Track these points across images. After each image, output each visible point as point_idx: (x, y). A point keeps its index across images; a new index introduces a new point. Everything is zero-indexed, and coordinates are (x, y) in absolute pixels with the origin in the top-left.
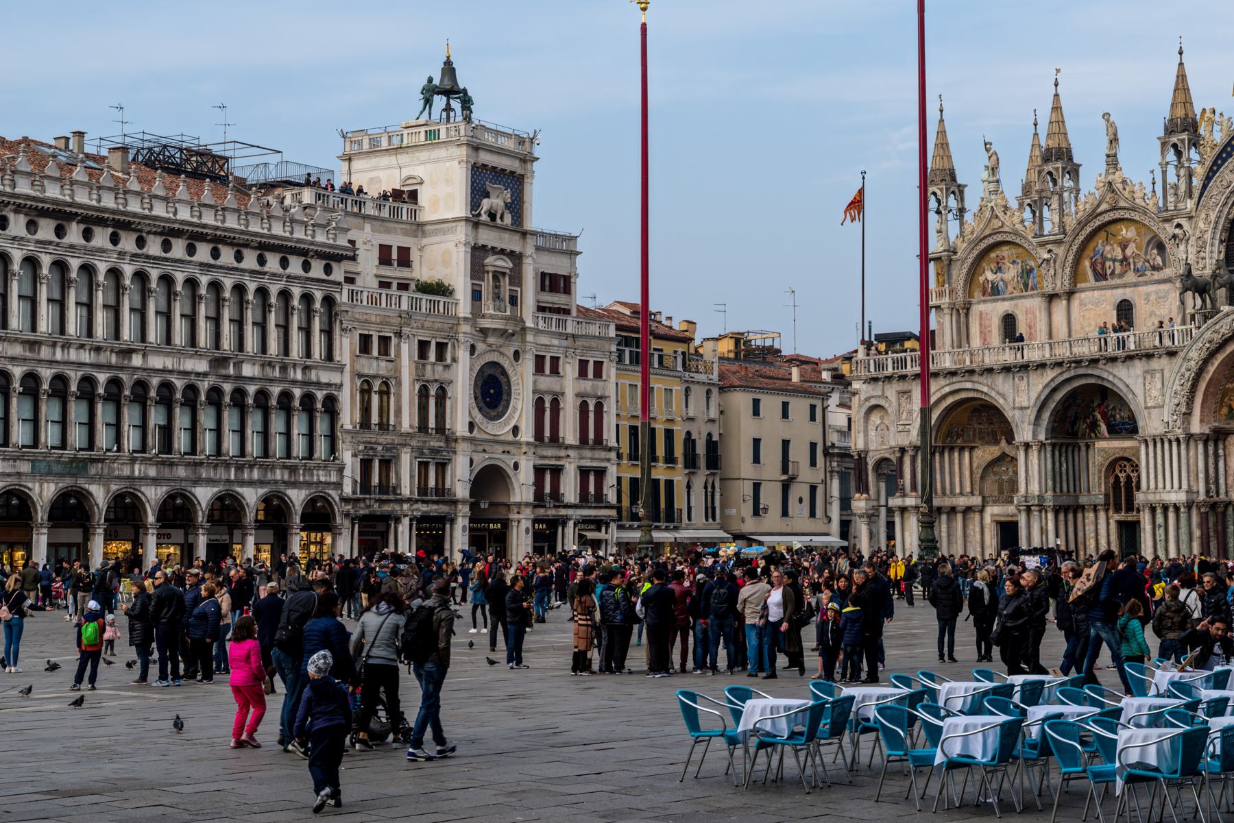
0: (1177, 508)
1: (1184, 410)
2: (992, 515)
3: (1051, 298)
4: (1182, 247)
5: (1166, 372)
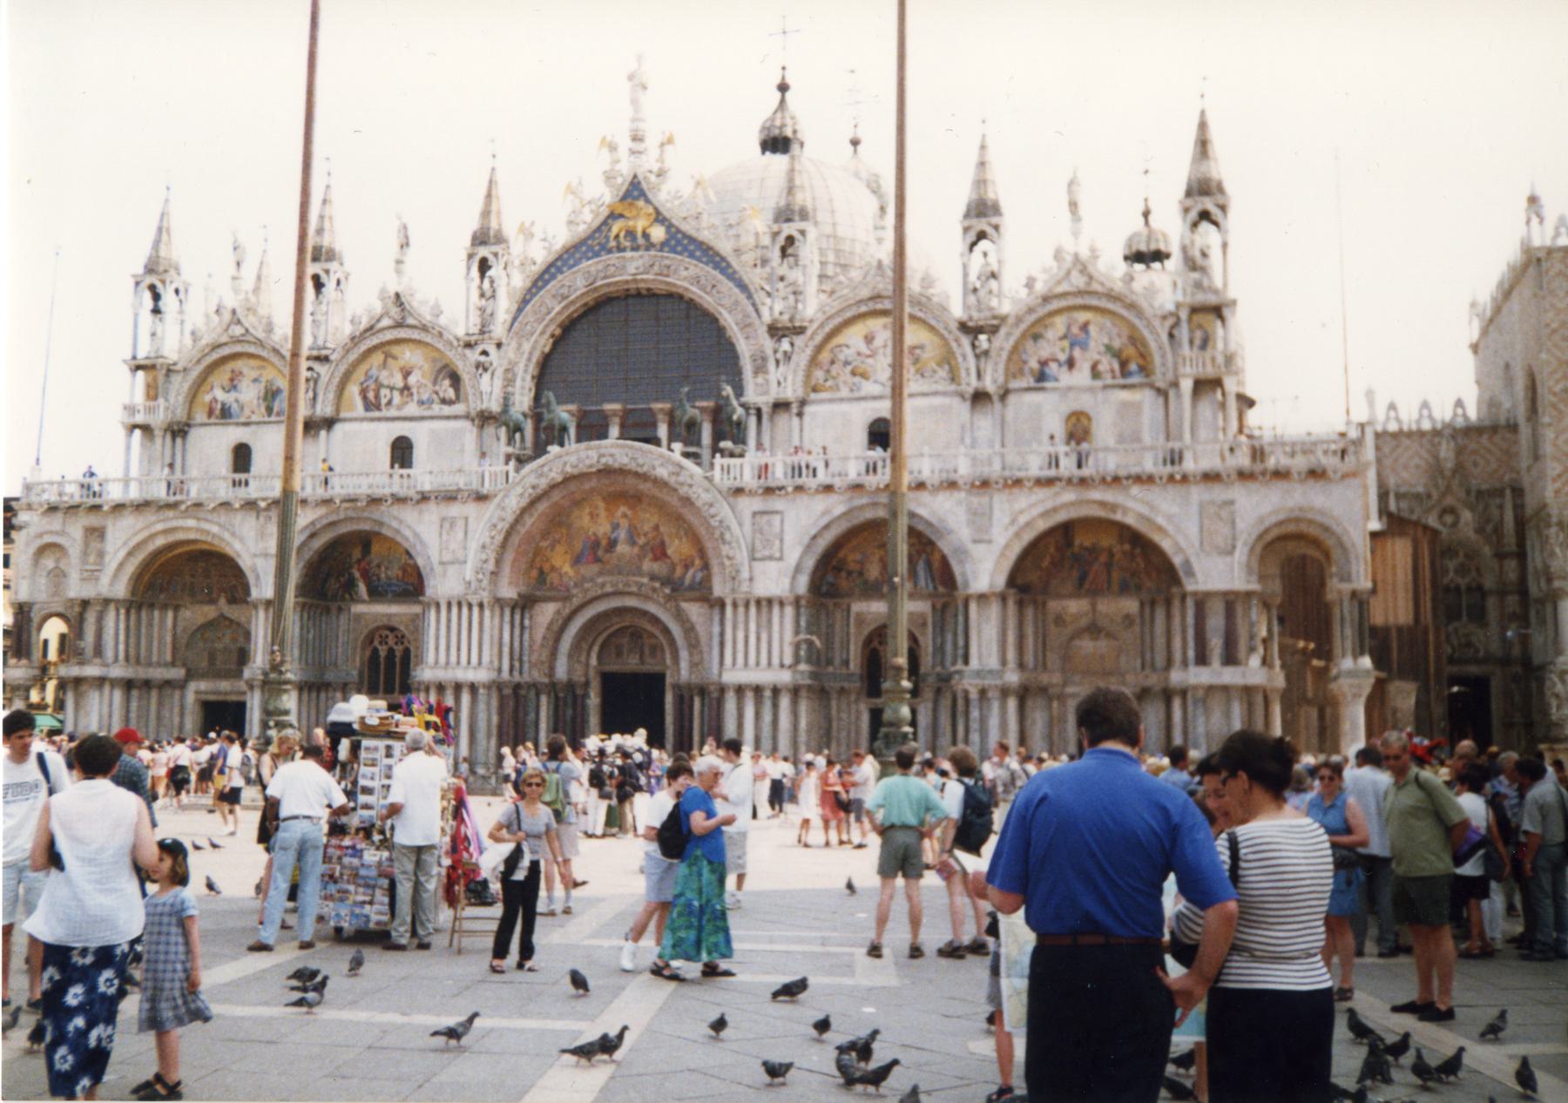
0: (473, 688)
1: (491, 566)
2: (197, 692)
4: (486, 377)
5: (471, 521)
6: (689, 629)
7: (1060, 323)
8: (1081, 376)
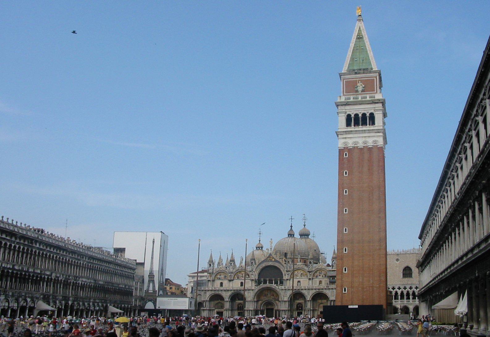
0: (252, 310)
1: (254, 297)
3: (230, 281)
4: (252, 276)
6: (277, 304)
7: (319, 271)
8: (321, 277)
